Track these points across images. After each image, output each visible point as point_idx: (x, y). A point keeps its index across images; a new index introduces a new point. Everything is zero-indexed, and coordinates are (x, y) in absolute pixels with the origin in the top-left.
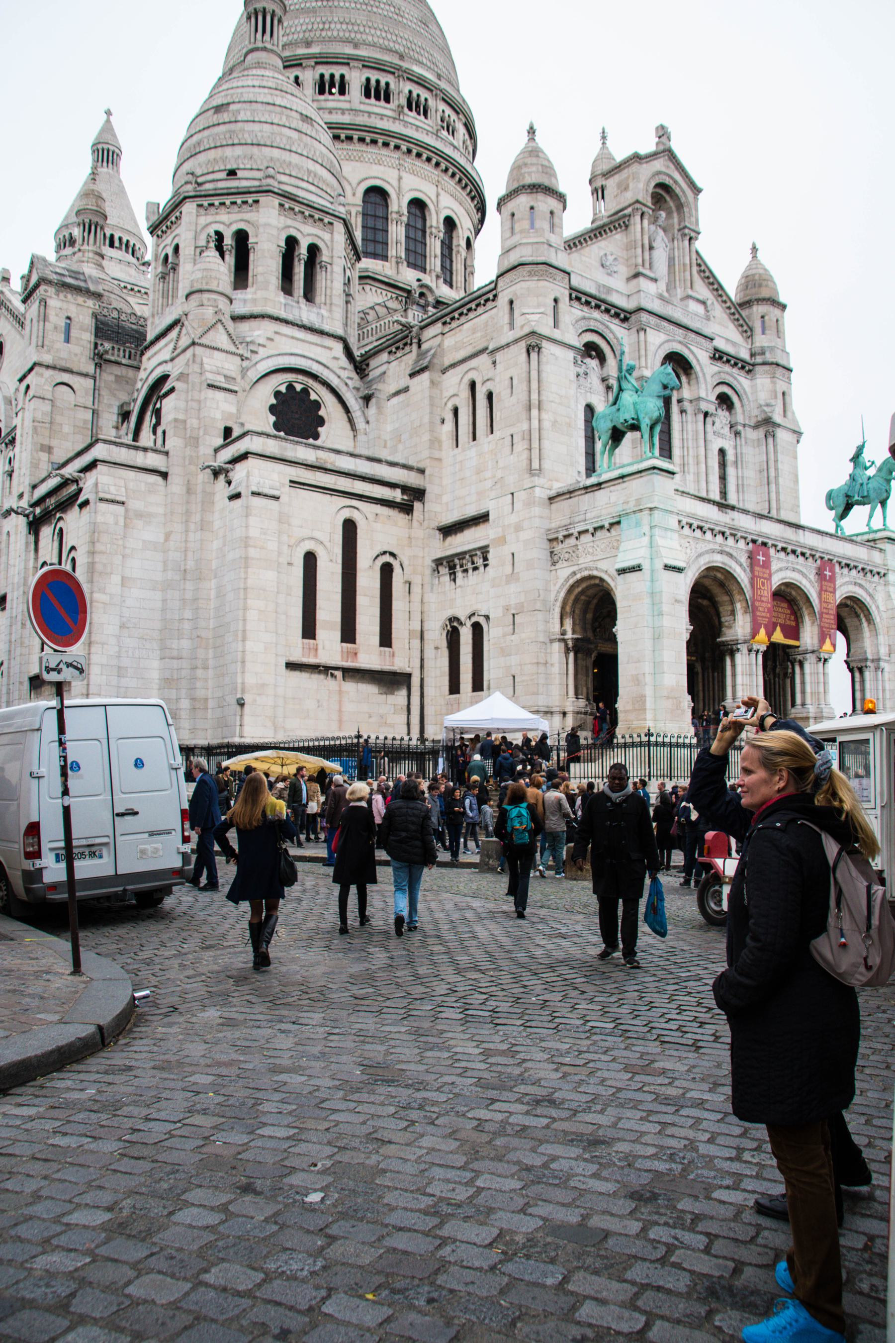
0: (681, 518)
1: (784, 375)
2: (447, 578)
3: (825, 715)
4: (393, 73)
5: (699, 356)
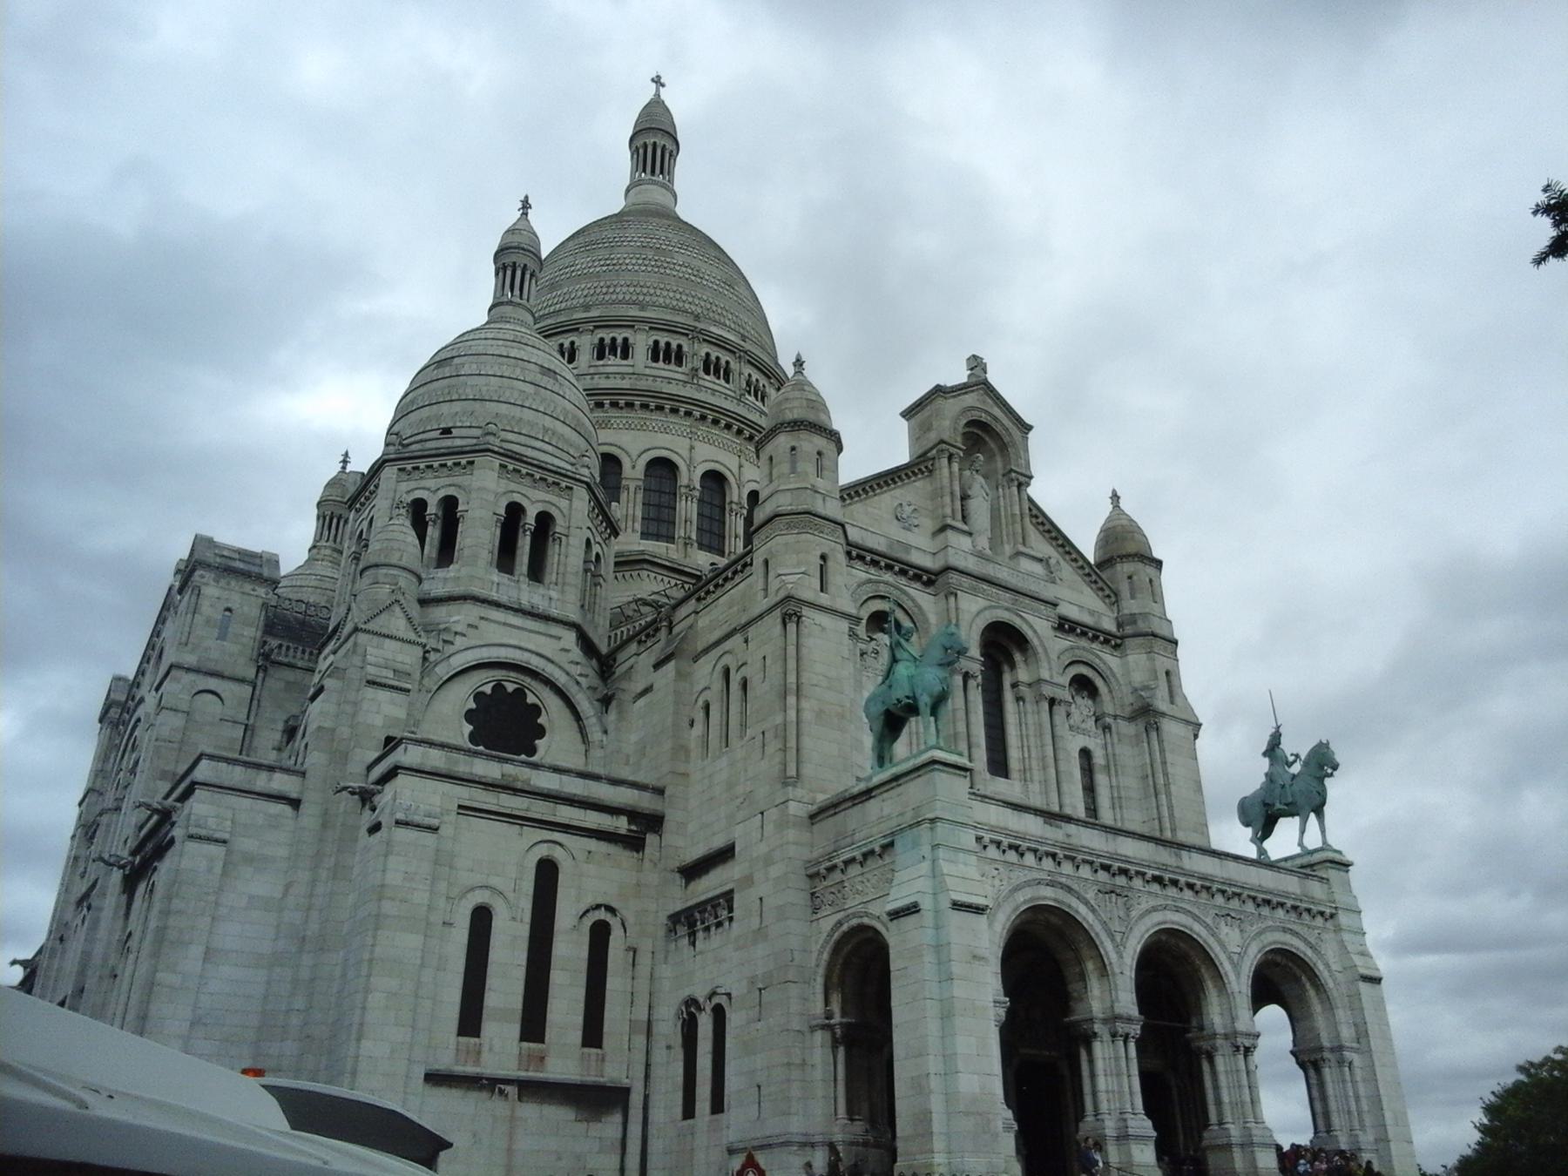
0: (981, 833)
1: (1165, 649)
2: (686, 941)
3: (1255, 1139)
4: (687, 335)
5: (1037, 626)
